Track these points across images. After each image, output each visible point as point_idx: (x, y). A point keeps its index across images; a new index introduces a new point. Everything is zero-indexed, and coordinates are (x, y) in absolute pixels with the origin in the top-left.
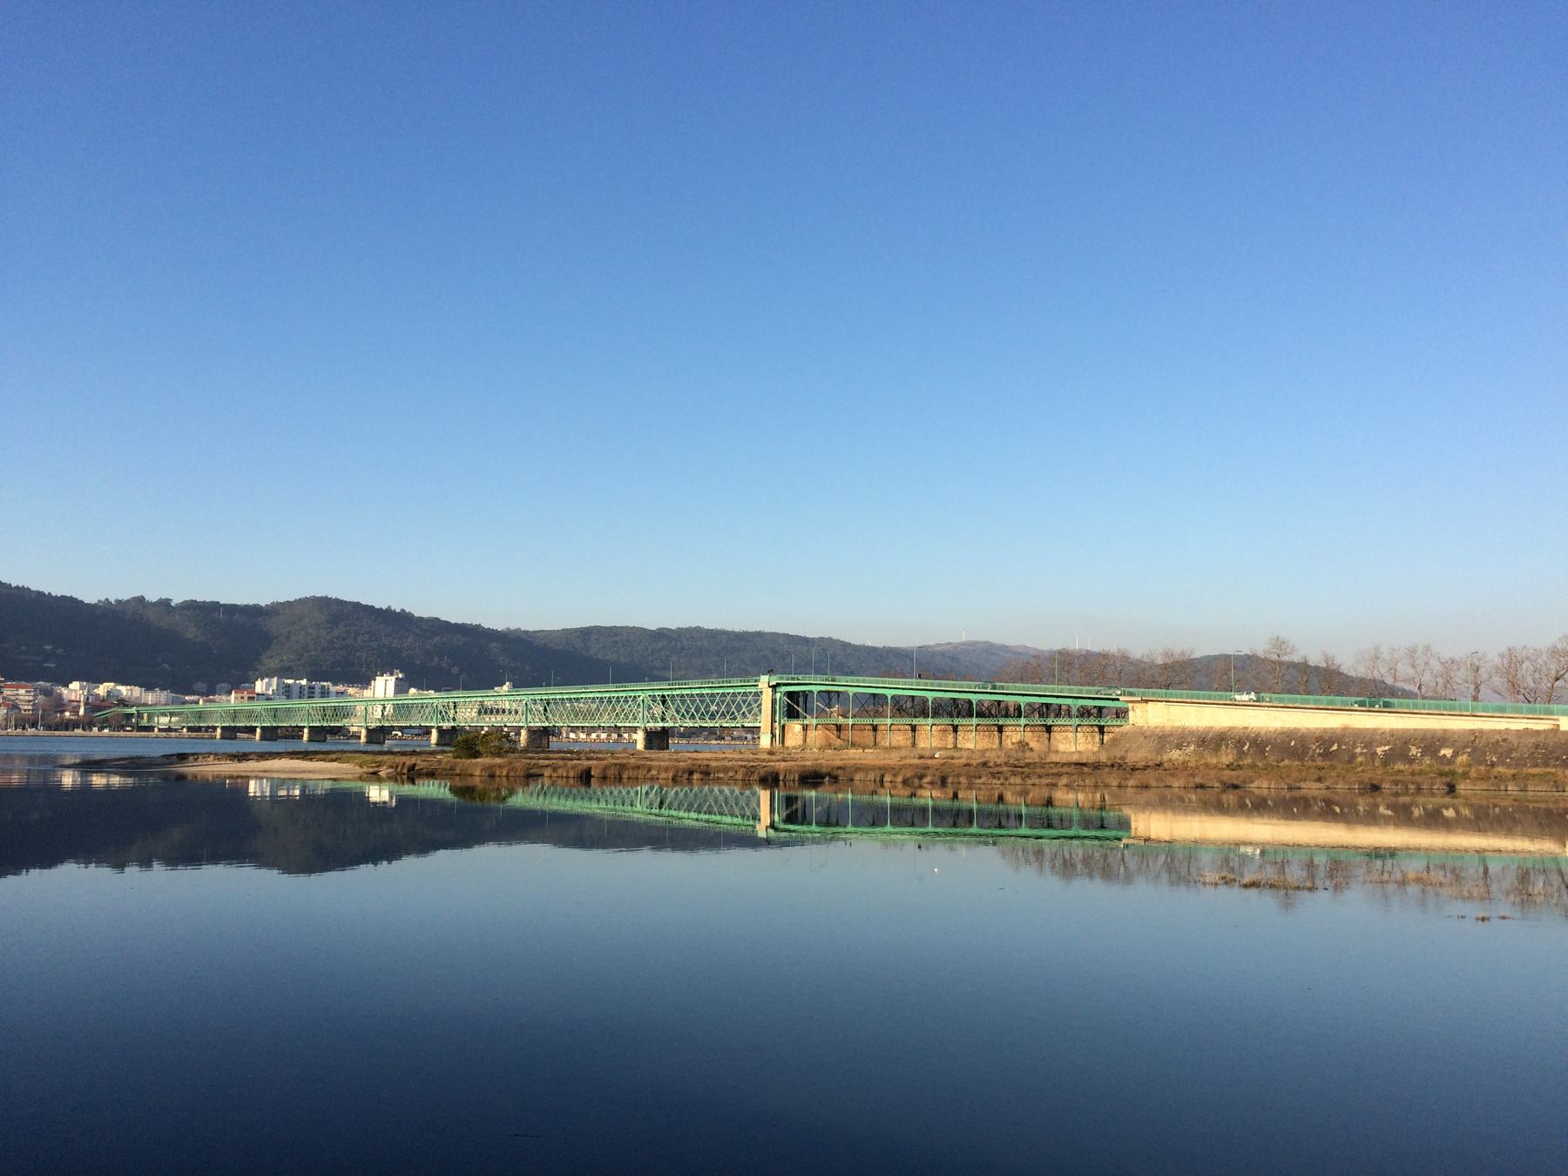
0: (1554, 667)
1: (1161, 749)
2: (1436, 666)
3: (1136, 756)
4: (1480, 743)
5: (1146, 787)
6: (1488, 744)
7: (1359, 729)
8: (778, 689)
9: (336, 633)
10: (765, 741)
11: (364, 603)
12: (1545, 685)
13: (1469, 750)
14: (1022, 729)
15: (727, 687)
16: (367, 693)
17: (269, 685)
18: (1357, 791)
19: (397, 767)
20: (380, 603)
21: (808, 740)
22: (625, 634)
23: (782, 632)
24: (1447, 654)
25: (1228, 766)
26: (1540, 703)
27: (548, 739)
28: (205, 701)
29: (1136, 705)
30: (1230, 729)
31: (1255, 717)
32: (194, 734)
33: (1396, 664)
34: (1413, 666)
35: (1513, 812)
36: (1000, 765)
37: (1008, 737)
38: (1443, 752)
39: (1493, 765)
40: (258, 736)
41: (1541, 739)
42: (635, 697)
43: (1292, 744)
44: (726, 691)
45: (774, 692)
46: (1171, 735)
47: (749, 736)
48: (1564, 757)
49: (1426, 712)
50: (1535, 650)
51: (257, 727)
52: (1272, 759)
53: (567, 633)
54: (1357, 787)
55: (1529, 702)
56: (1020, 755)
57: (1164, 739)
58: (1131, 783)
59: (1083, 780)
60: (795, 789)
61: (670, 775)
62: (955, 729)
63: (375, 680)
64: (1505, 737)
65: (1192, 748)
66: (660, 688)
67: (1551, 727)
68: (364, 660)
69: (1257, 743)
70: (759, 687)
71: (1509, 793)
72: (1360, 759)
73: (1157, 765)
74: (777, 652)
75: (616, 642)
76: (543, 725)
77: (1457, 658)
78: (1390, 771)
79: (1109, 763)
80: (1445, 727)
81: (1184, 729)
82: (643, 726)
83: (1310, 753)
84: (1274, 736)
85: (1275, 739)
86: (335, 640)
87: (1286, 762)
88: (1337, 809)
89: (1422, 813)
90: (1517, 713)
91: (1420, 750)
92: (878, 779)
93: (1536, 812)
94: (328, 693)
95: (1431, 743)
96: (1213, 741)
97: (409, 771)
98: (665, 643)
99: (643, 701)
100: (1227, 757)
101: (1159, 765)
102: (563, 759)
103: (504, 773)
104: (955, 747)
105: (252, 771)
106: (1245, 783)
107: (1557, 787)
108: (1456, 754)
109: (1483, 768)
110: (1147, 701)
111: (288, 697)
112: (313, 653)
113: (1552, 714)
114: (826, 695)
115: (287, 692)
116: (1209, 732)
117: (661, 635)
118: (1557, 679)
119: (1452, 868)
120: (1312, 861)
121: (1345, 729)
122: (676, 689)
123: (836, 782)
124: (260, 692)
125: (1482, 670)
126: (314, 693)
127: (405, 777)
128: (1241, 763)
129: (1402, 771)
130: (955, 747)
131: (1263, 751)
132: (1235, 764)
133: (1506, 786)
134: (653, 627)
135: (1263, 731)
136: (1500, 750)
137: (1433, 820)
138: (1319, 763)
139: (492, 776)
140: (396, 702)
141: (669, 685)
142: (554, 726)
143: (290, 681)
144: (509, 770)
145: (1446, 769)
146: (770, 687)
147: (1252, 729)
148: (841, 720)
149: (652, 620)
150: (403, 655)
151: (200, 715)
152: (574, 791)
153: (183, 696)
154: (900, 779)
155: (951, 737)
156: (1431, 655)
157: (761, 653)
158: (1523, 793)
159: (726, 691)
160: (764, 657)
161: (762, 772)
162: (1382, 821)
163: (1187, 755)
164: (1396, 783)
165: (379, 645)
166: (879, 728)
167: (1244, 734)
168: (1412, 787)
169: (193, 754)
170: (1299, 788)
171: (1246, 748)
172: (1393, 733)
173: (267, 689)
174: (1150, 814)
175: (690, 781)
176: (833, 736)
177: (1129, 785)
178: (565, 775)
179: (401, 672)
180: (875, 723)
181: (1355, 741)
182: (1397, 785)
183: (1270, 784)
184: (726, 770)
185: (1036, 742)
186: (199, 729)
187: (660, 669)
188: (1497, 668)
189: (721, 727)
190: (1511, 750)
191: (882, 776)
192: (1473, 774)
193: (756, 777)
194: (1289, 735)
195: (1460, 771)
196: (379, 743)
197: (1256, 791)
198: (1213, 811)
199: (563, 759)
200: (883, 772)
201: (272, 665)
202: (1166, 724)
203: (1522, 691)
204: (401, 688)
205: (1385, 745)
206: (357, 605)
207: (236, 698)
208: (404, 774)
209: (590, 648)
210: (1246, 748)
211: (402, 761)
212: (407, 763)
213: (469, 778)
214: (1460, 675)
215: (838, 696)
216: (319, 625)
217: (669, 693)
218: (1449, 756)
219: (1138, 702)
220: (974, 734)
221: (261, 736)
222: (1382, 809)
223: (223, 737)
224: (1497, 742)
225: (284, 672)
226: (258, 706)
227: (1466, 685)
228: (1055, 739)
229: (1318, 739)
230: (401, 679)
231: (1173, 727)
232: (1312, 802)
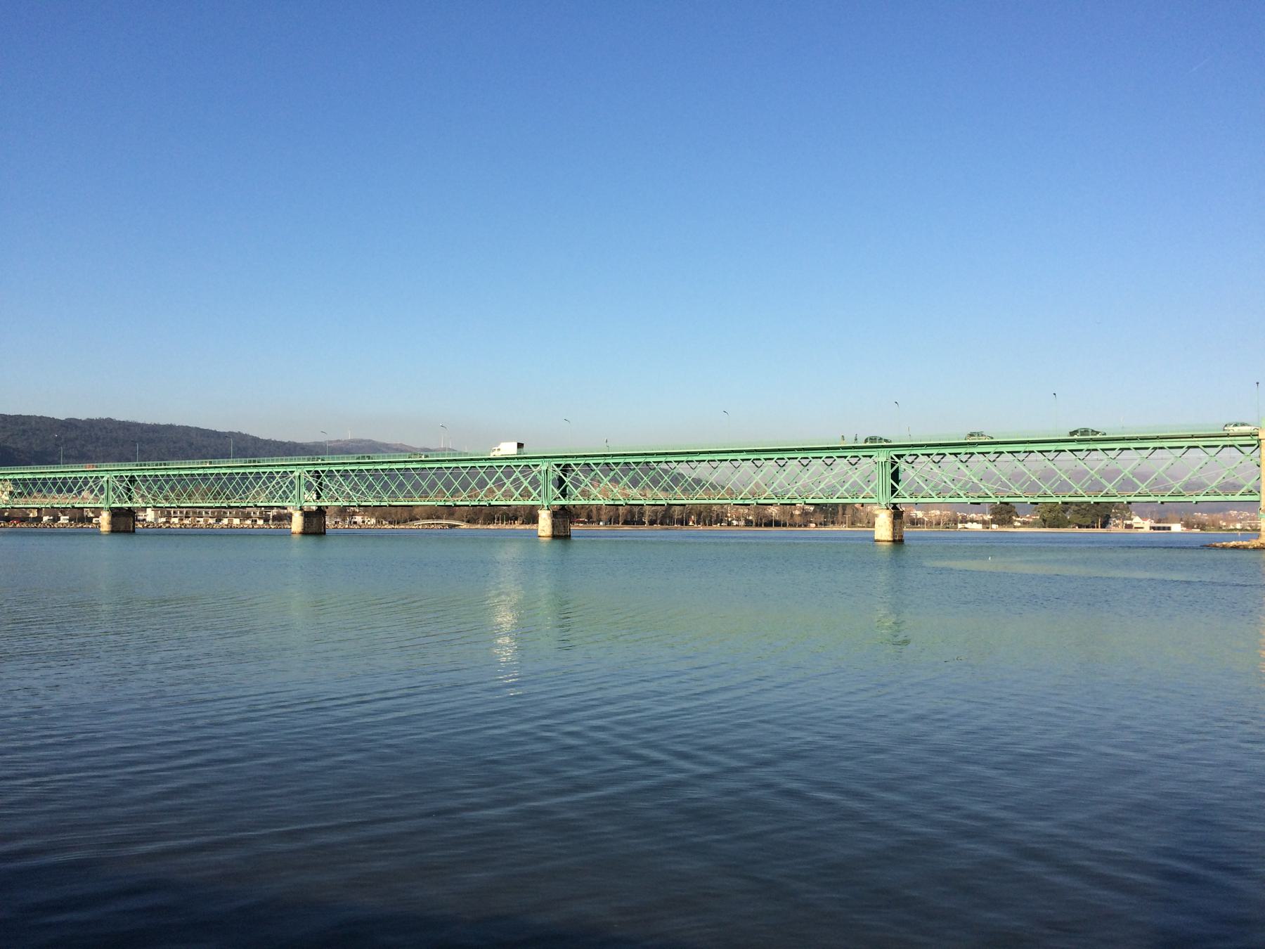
15: (278, 466)
22: (33, 423)
42: (97, 477)
66: (129, 469)
75: (24, 431)
82: (546, 505)
99: (108, 481)
134: (61, 415)
141: (137, 465)
149: (60, 411)
160: (180, 449)
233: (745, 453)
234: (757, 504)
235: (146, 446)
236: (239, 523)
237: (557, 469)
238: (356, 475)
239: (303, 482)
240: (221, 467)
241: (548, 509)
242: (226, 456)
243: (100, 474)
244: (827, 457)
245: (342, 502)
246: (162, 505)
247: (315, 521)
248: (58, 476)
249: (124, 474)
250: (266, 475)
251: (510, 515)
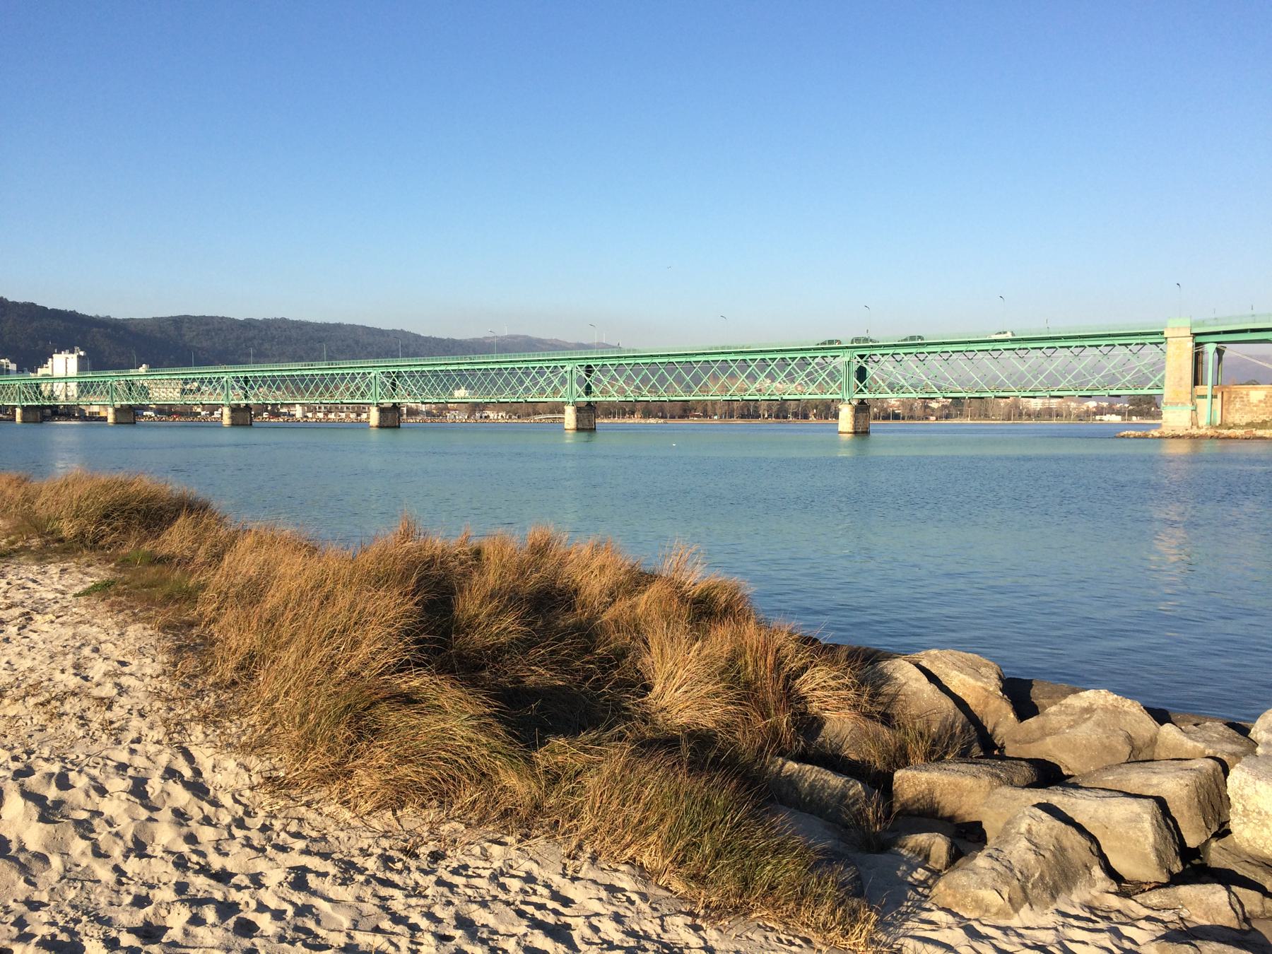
10: (1175, 418)
16: (41, 371)
40: (18, 418)
63: (52, 358)
70: (1165, 336)
75: (208, 331)
76: (129, 403)
82: (847, 399)
134: (241, 316)
149: (239, 311)
160: (348, 346)
189: (499, 402)
196: (247, 425)
204: (82, 368)
209: (184, 335)
233: (1009, 342)
234: (1109, 396)
237: (860, 360)
238: (551, 372)
239: (575, 376)
241: (850, 404)
242: (415, 355)
243: (367, 371)
244: (1048, 348)
245: (617, 398)
246: (430, 401)
250: (795, 361)
251: (803, 411)
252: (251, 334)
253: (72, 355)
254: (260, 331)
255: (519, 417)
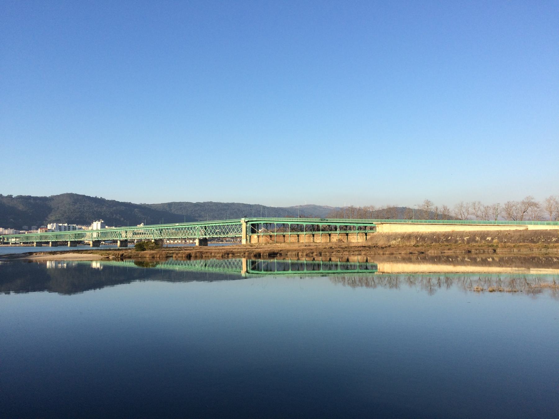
0: (523, 208)
1: (389, 241)
2: (482, 209)
3: (381, 243)
4: (500, 235)
5: (393, 254)
6: (503, 235)
7: (458, 231)
8: (248, 223)
9: (76, 206)
10: (244, 242)
11: (86, 195)
12: (519, 216)
13: (497, 237)
14: (357, 234)
16: (90, 228)
17: (53, 226)
18: (464, 253)
19: (116, 255)
20: (92, 195)
21: (259, 241)
22: (184, 205)
23: (241, 203)
24: (486, 205)
25: (414, 246)
26: (518, 220)
27: (207, 243)
28: (27, 233)
29: (379, 225)
30: (413, 233)
31: (421, 228)
32: (25, 245)
33: (468, 208)
34: (475, 209)
35: (512, 259)
36: (337, 248)
37: (332, 238)
38: (488, 238)
39: (505, 242)
40: (50, 245)
41: (522, 233)
43: (435, 237)
44: (229, 224)
45: (247, 224)
46: (392, 235)
47: (232, 240)
48: (530, 239)
49: (482, 225)
50: (517, 202)
51: (50, 242)
52: (429, 242)
53: (163, 205)
54: (464, 251)
55: (515, 220)
56: (340, 244)
57: (389, 237)
58: (387, 253)
59: (370, 252)
60: (267, 259)
61: (221, 255)
62: (313, 235)
63: (93, 223)
64: (509, 233)
65: (399, 240)
67: (525, 229)
68: (87, 216)
69: (422, 237)
70: (241, 222)
71: (514, 252)
72: (460, 242)
73: (389, 246)
74: (240, 210)
75: (181, 208)
77: (489, 206)
78: (471, 246)
79: (373, 246)
80: (488, 230)
81: (396, 233)
83: (441, 240)
84: (428, 235)
85: (429, 236)
86: (76, 209)
87: (434, 243)
88: (451, 259)
89: (481, 260)
90: (512, 224)
91: (480, 238)
92: (296, 254)
93: (520, 259)
94: (76, 228)
95: (483, 235)
96: (408, 237)
97: (121, 256)
98: (199, 208)
100: (413, 243)
101: (390, 246)
102: (177, 250)
103: (158, 256)
104: (314, 242)
105: (60, 258)
106: (425, 251)
107: (531, 249)
108: (492, 239)
109: (502, 244)
110: (383, 224)
111: (60, 230)
112: (68, 214)
113: (526, 224)
114: (265, 225)
115: (60, 228)
116: (404, 235)
117: (198, 204)
118: (524, 212)
119: (487, 279)
120: (500, 279)
121: (453, 231)
122: (210, 224)
123: (281, 256)
124: (49, 229)
125: (498, 210)
126: (70, 228)
127: (119, 259)
128: (418, 244)
129: (475, 246)
130: (314, 242)
131: (425, 240)
132: (416, 245)
133: (513, 250)
134: (195, 202)
135: (424, 233)
136: (508, 237)
137: (484, 262)
138: (446, 244)
139: (153, 257)
140: (101, 231)
142: (220, 237)
143: (61, 225)
144: (160, 255)
145: (490, 244)
146: (245, 222)
147: (420, 232)
148: (272, 234)
149: (194, 200)
150: (102, 214)
151: (27, 238)
152: (185, 262)
153: (19, 231)
154: (305, 254)
155: (312, 239)
156: (481, 205)
157: (234, 211)
158: (519, 252)
159: (229, 224)
160: (235, 212)
161: (255, 252)
162: (466, 263)
163: (398, 242)
164: (476, 250)
165: (93, 211)
166: (315, 235)
167: (418, 234)
168: (482, 251)
169: (35, 252)
170: (444, 253)
171: (418, 239)
172: (470, 232)
173: (52, 228)
174: (384, 263)
175: (228, 257)
176: (269, 239)
177: (387, 253)
178: (181, 256)
179: (103, 220)
180: (284, 234)
181: (456, 236)
182: (477, 250)
183: (435, 251)
184: (240, 252)
185: (344, 239)
186: (27, 243)
187: (198, 217)
188: (503, 208)
190: (511, 237)
191: (298, 253)
192: (500, 246)
193: (252, 255)
194: (433, 234)
195: (495, 245)
196: (97, 246)
197: (430, 254)
198: (407, 261)
199: (177, 250)
200: (298, 251)
201: (52, 218)
202: (390, 232)
203: (512, 217)
204: (103, 226)
205: (467, 237)
206: (84, 196)
207: (40, 231)
208: (119, 257)
209: (172, 210)
210: (418, 239)
211: (118, 253)
212: (120, 253)
213: (144, 259)
214: (491, 212)
215: (270, 225)
216: (70, 204)
217: (208, 225)
218: (490, 240)
219: (380, 224)
220: (338, 236)
221: (51, 245)
222: (466, 259)
223: (37, 246)
224: (507, 234)
225: (57, 221)
226: (50, 234)
227: (493, 215)
228: (350, 238)
229: (444, 235)
230: (103, 223)
231: (392, 233)
232: (442, 257)
235: (223, 212)
236: (173, 242)
240: (220, 223)
247: (124, 243)
248: (189, 226)
249: (203, 226)
252: (197, 209)
253: (99, 222)
254: (201, 207)
255: (226, 241)
